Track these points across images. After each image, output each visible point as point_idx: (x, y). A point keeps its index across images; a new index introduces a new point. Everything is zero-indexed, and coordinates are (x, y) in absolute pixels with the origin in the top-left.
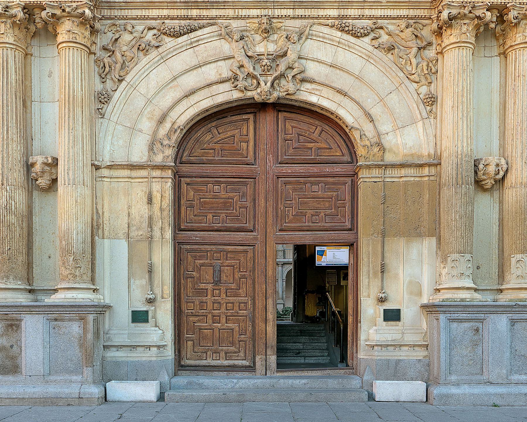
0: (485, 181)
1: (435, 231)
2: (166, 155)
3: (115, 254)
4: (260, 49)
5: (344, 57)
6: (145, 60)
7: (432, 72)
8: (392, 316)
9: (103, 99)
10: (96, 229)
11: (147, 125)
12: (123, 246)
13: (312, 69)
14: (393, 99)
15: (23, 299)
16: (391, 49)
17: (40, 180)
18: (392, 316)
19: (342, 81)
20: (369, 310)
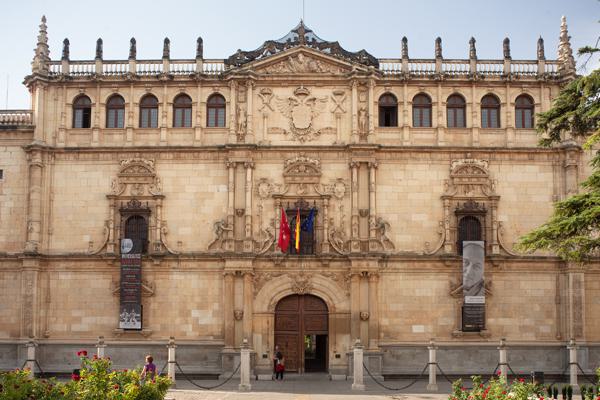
0: (363, 318)
1: (349, 332)
2: (272, 310)
3: (258, 338)
4: (300, 280)
5: (326, 283)
6: (267, 283)
7: (349, 287)
8: (338, 356)
9: (255, 294)
10: (253, 331)
11: (267, 301)
12: (260, 336)
13: (315, 286)
14: (338, 294)
15: (234, 351)
16: (336, 280)
17: (238, 317)
18: (338, 356)
19: (324, 289)
20: (331, 354)
